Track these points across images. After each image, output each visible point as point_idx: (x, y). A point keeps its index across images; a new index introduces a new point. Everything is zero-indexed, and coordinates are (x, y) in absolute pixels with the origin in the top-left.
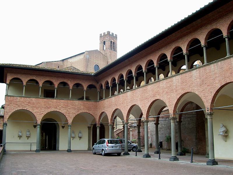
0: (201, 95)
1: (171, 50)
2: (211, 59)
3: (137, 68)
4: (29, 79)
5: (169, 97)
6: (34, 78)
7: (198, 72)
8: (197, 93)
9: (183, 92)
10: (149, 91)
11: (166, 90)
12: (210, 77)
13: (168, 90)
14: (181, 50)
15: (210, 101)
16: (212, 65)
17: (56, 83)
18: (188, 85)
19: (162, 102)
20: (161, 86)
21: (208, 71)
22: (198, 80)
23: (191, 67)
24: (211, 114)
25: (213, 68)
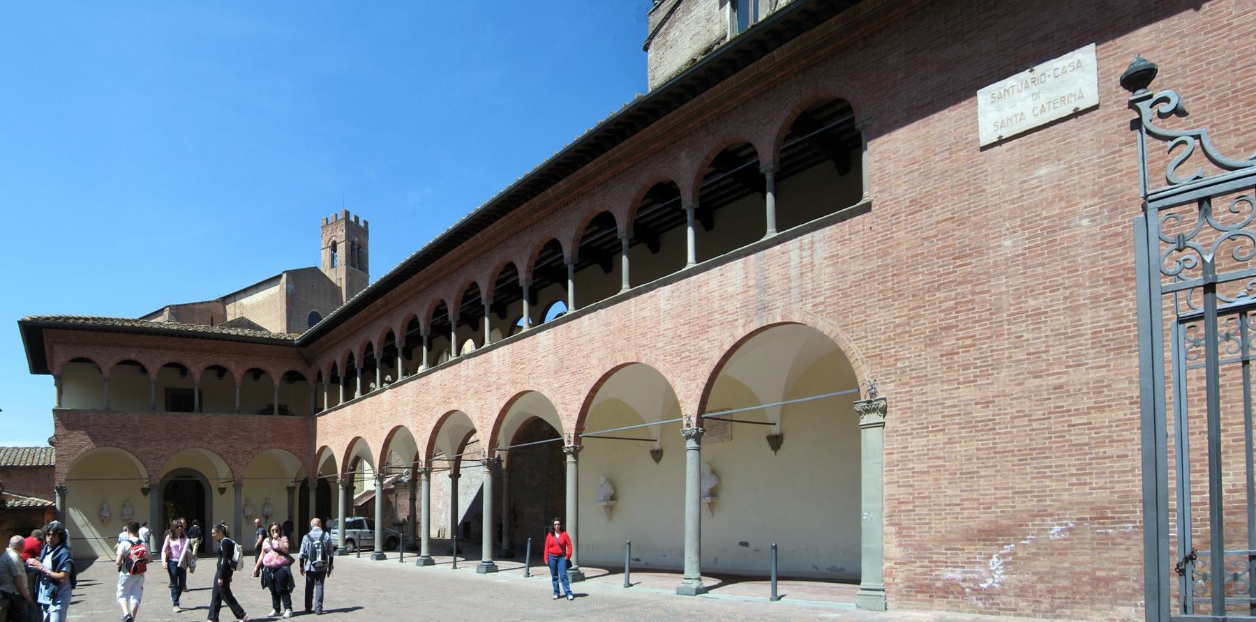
0: (556, 400)
1: (489, 271)
2: (589, 299)
3: (407, 324)
4: (118, 359)
5: (480, 403)
6: (133, 356)
7: (551, 335)
8: (546, 393)
9: (514, 392)
10: (434, 388)
11: (475, 385)
12: (580, 350)
13: (479, 384)
14: (516, 273)
15: (576, 416)
16: (586, 317)
17: (197, 367)
18: (527, 371)
19: (465, 417)
20: (463, 373)
21: (574, 333)
22: (551, 358)
23: (539, 320)
24: (575, 453)
25: (587, 323)
